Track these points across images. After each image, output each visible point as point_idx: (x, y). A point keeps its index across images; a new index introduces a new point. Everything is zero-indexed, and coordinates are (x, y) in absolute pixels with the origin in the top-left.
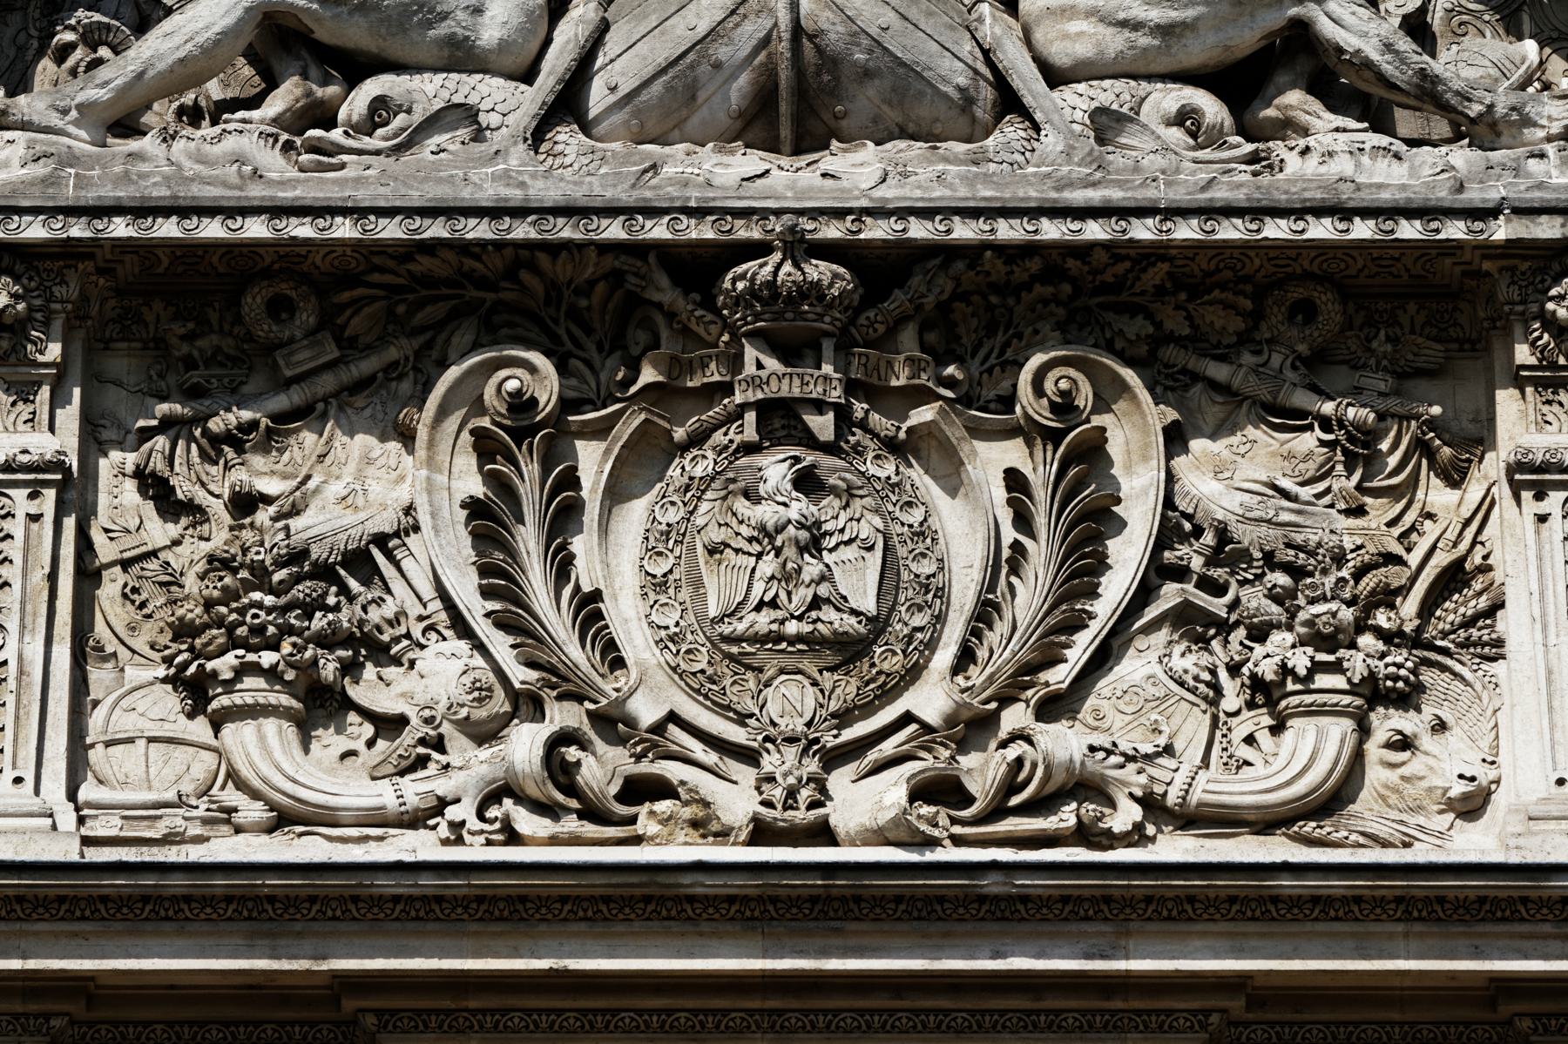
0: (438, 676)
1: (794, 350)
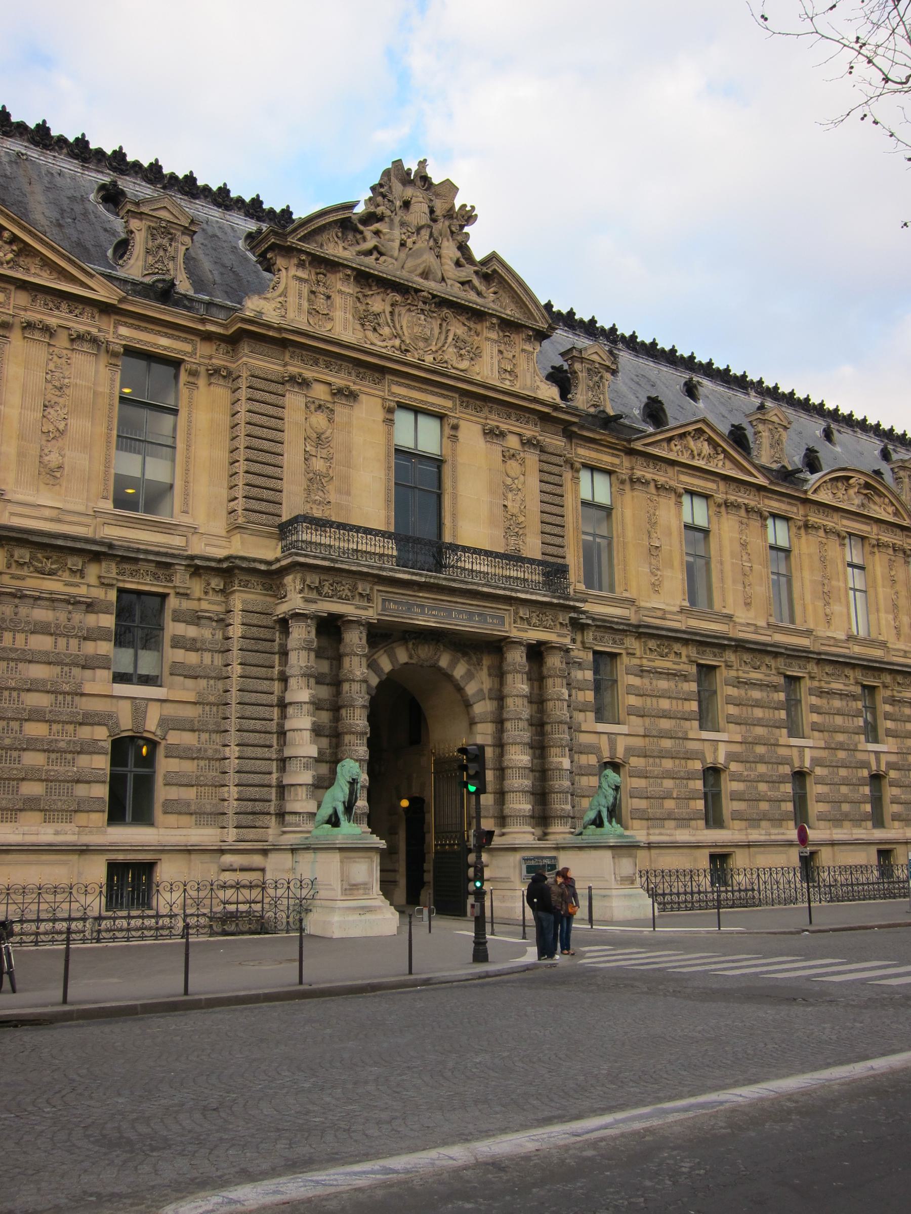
0: (386, 331)
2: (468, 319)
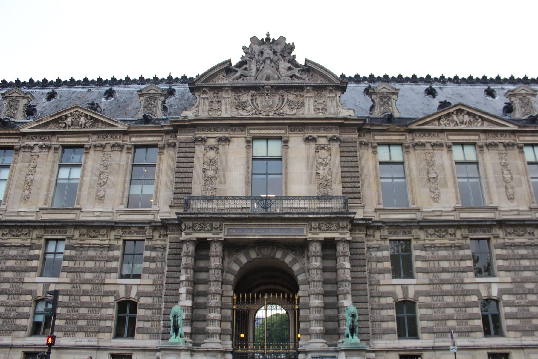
1: (268, 91)
2: (295, 91)
